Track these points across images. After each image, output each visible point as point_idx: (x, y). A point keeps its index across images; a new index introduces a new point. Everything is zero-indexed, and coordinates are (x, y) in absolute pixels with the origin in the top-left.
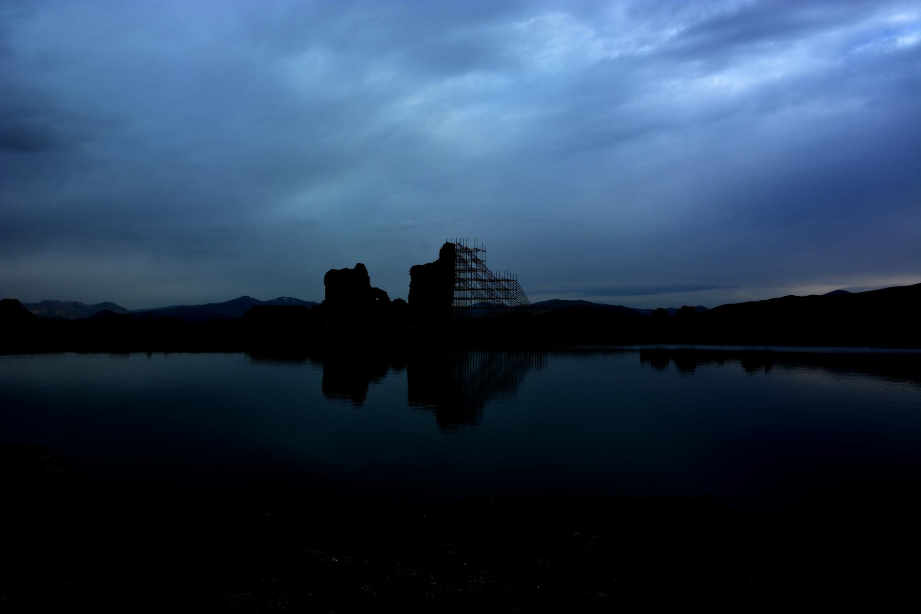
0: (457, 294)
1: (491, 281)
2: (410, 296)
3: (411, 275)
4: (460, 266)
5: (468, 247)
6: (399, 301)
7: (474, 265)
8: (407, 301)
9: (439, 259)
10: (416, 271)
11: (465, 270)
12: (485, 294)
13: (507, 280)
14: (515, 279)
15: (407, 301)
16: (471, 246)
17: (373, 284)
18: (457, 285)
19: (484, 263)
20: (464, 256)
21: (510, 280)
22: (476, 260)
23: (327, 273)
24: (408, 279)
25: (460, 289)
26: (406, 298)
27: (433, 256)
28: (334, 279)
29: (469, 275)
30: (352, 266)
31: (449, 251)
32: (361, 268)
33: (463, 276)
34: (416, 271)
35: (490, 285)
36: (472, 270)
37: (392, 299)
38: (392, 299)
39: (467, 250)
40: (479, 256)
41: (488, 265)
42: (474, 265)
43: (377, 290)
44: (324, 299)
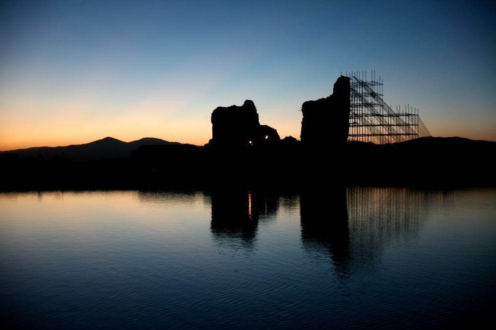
0: (352, 130)
1: (390, 116)
2: (301, 136)
3: (303, 111)
4: (355, 101)
5: (364, 81)
6: (290, 139)
7: (370, 99)
8: (299, 139)
9: (333, 94)
10: (308, 108)
11: (361, 105)
12: (401, 130)
13: (407, 115)
14: (417, 114)
15: (299, 139)
16: (368, 80)
17: (262, 122)
18: (351, 121)
19: (381, 97)
20: (360, 90)
21: (411, 115)
22: (373, 95)
23: (214, 111)
24: (300, 116)
25: (355, 125)
26: (297, 134)
27: (325, 91)
28: (220, 117)
29: (366, 110)
30: (240, 103)
31: (343, 85)
32: (249, 105)
33: (359, 111)
34: (308, 108)
35: (392, 121)
36: (367, 105)
37: (282, 137)
38: (282, 137)
39: (363, 84)
40: (376, 89)
41: (386, 99)
42: (370, 99)
43: (266, 127)
44: (211, 138)
